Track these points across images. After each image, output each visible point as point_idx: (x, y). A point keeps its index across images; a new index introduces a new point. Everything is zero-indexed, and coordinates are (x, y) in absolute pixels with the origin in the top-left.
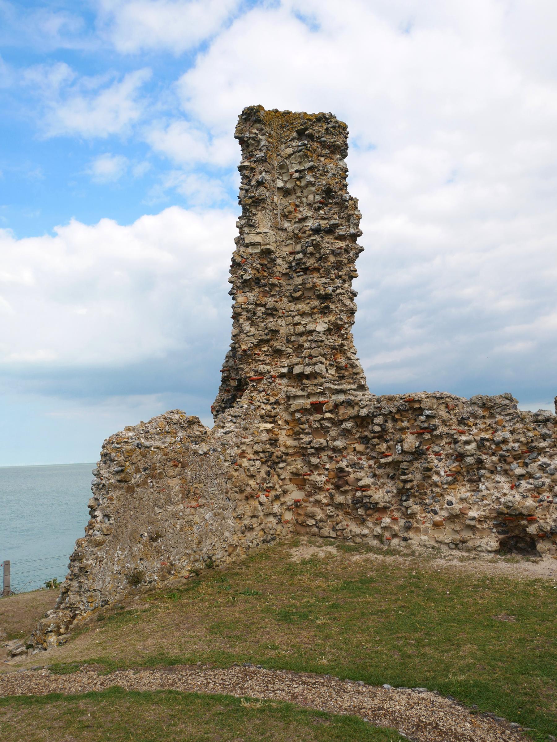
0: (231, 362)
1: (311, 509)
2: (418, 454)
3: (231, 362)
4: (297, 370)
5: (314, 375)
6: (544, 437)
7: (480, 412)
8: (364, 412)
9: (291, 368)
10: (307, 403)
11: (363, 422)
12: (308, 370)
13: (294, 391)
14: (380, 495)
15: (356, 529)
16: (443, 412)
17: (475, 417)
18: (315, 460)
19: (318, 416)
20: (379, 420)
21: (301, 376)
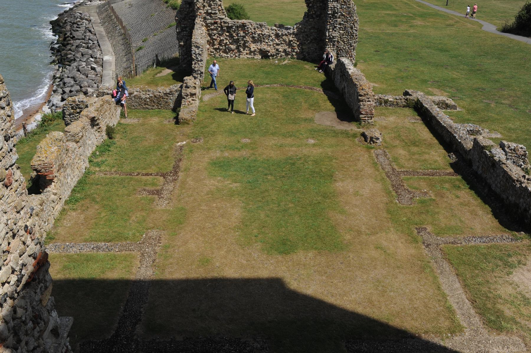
0: (184, 6)
1: (212, 50)
2: (244, 37)
3: (184, 6)
4: (210, 11)
5: (215, 14)
6: (273, 33)
7: (259, 27)
8: (230, 25)
9: (207, 10)
10: (213, 21)
11: (228, 27)
12: (213, 12)
13: (209, 17)
14: (233, 47)
15: (226, 55)
16: (250, 26)
17: (258, 27)
18: (214, 37)
19: (216, 25)
20: (234, 27)
21: (211, 13)
